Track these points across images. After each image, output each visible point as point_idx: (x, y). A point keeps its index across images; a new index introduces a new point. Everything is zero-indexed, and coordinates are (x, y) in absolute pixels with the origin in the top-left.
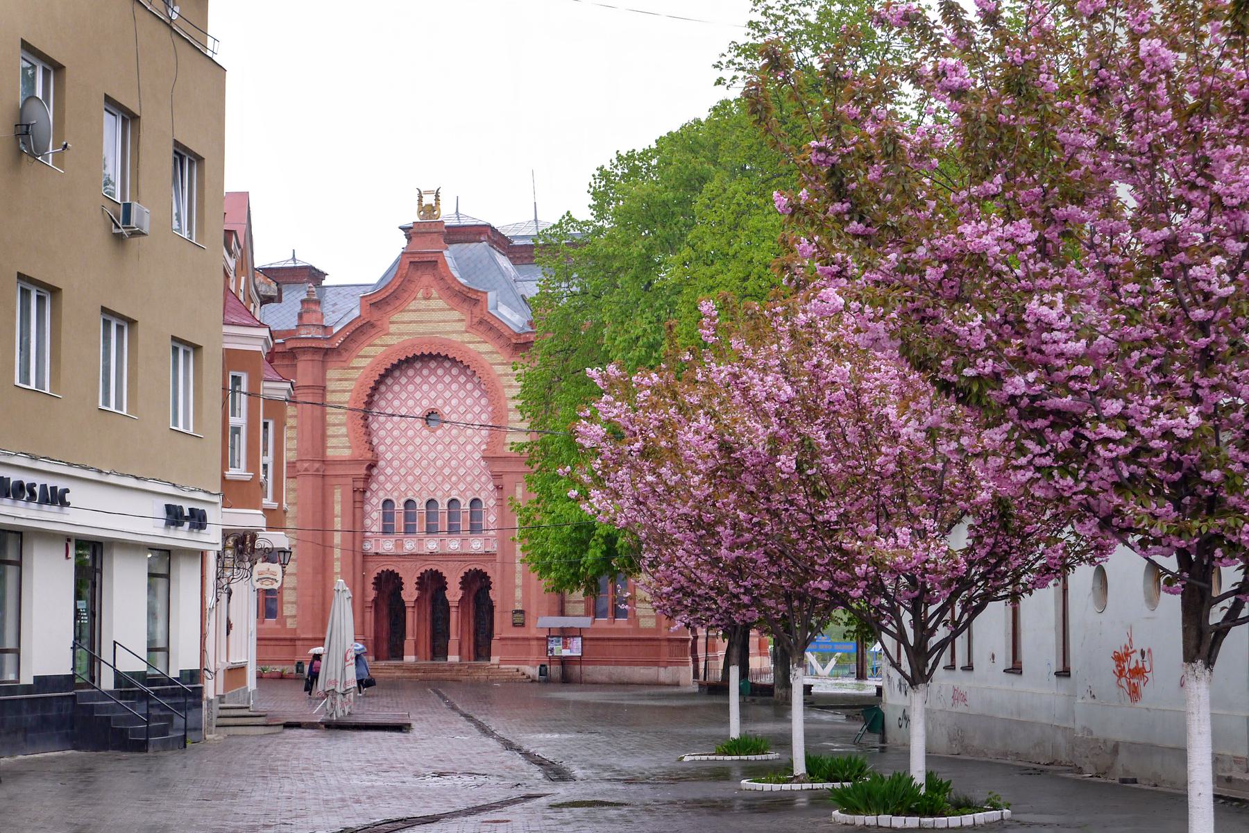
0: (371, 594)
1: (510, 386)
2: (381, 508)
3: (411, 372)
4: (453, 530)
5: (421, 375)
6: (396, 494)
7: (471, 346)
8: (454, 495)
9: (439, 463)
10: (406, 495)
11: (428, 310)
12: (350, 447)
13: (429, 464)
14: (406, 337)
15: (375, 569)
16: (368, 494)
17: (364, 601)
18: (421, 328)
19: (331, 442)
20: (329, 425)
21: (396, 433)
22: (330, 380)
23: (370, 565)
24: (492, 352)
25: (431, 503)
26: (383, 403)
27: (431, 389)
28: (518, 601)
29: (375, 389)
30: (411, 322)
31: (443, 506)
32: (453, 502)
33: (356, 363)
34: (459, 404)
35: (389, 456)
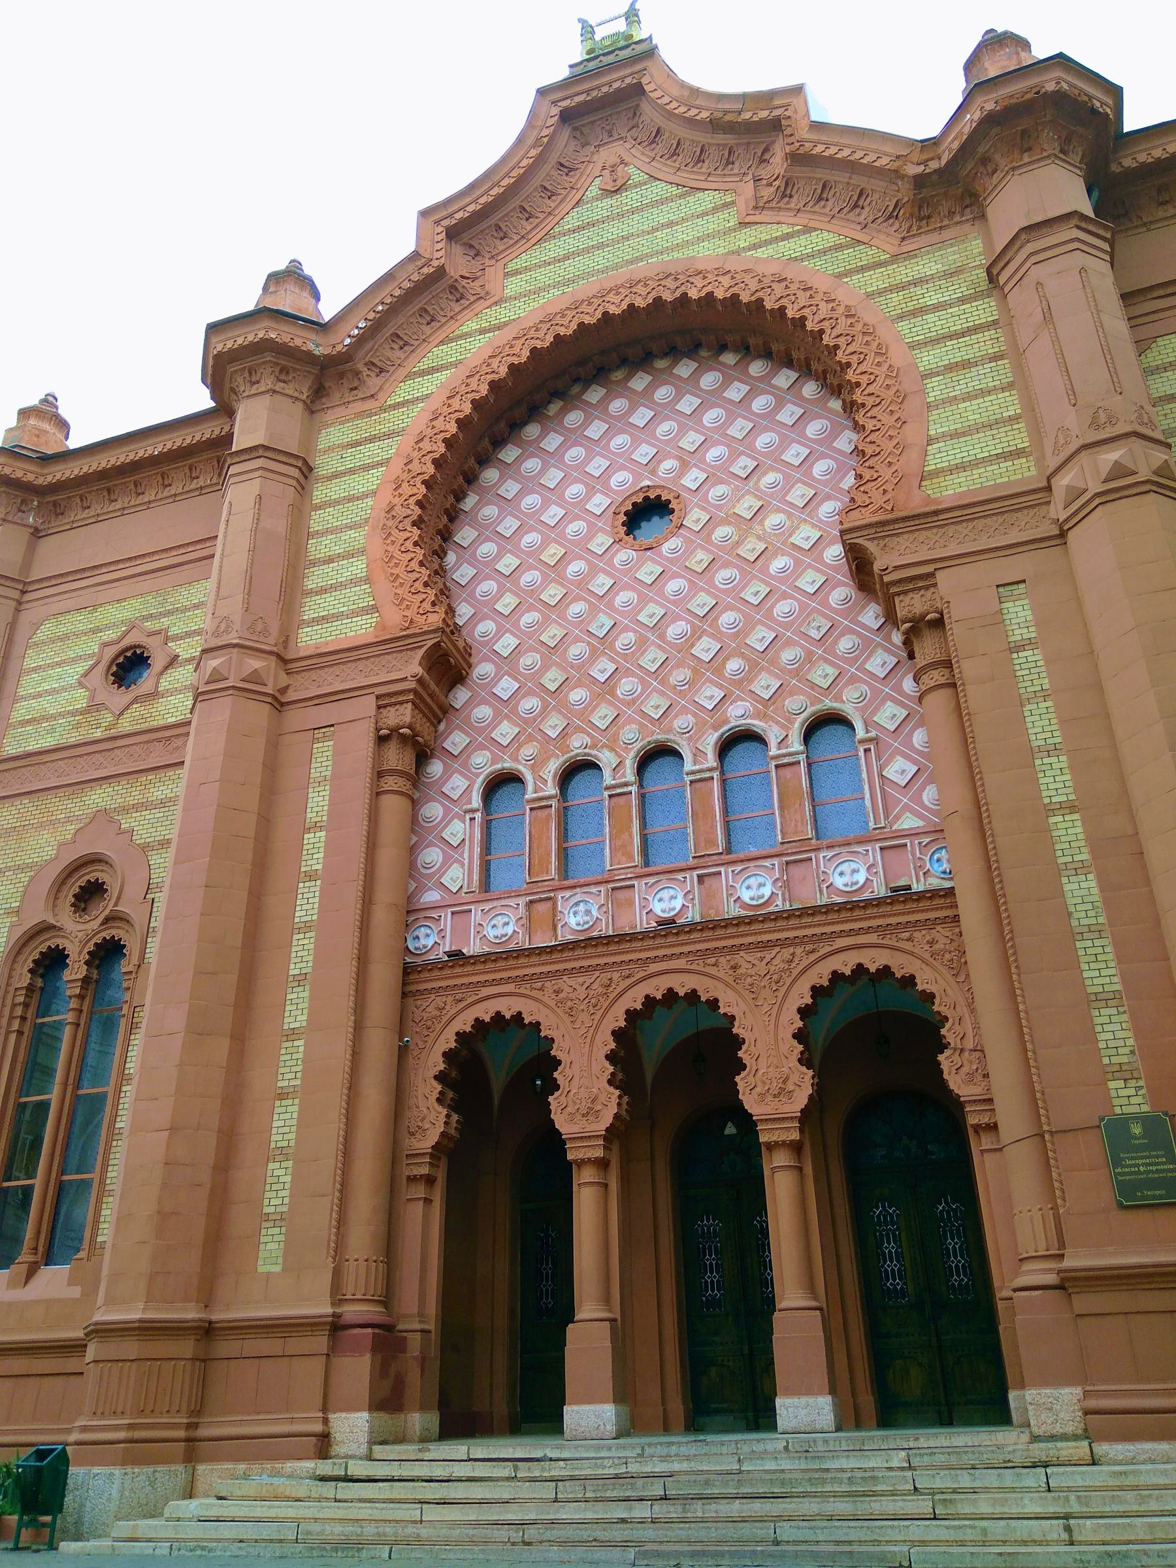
2: (476, 801)
3: (573, 418)
5: (605, 415)
6: (528, 751)
7: (761, 253)
8: (738, 714)
9: (675, 630)
10: (565, 749)
12: (375, 608)
16: (436, 768)
18: (600, 259)
19: (312, 608)
22: (330, 449)
23: (427, 1007)
24: (839, 248)
28: (1125, 1074)
30: (566, 257)
33: (403, 391)
35: (506, 644)
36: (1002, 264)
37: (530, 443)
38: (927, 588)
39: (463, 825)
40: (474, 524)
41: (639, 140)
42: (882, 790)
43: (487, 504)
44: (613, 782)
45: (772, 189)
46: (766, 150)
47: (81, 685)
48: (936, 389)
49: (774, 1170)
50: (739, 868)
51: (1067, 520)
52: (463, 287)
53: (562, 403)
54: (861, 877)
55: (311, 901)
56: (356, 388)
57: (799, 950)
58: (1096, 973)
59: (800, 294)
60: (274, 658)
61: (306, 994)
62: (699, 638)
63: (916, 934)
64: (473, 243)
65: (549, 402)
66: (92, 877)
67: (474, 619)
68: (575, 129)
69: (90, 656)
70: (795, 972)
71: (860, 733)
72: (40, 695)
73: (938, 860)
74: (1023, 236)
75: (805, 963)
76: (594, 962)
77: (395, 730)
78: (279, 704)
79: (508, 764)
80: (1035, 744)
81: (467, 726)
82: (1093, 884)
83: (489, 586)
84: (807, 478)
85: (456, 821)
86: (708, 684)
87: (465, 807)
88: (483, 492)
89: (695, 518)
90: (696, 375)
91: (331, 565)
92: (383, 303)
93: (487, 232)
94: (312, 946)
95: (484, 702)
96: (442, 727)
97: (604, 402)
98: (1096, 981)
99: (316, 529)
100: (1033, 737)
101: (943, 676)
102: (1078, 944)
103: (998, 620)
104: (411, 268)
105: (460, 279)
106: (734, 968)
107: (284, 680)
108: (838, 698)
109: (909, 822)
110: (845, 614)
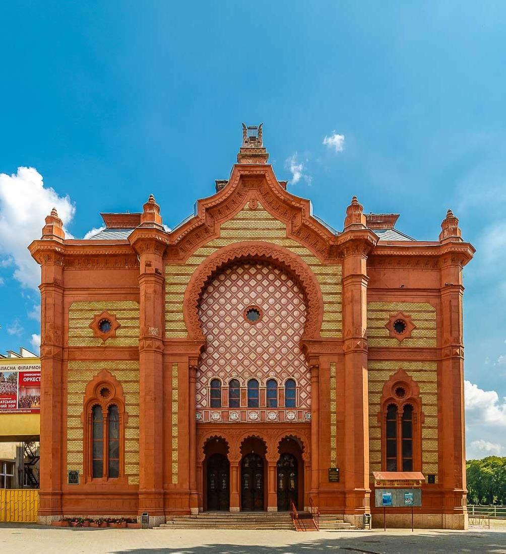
0: (203, 457)
2: (209, 385)
3: (234, 277)
4: (272, 405)
6: (222, 374)
8: (272, 375)
9: (259, 350)
13: (250, 350)
15: (206, 437)
16: (199, 374)
17: (197, 463)
21: (222, 325)
25: (253, 382)
26: (211, 301)
28: (333, 461)
29: (204, 290)
31: (262, 385)
32: (272, 382)
34: (275, 303)
35: (216, 343)
47: (90, 327)
49: (270, 471)
53: (230, 271)
62: (264, 353)
65: (228, 269)
66: (105, 387)
69: (92, 318)
71: (297, 385)
72: (76, 328)
81: (206, 364)
83: (210, 324)
84: (293, 316)
89: (265, 319)
90: (267, 275)
95: (210, 358)
96: (200, 363)
97: (242, 275)
106: (267, 432)
109: (304, 406)
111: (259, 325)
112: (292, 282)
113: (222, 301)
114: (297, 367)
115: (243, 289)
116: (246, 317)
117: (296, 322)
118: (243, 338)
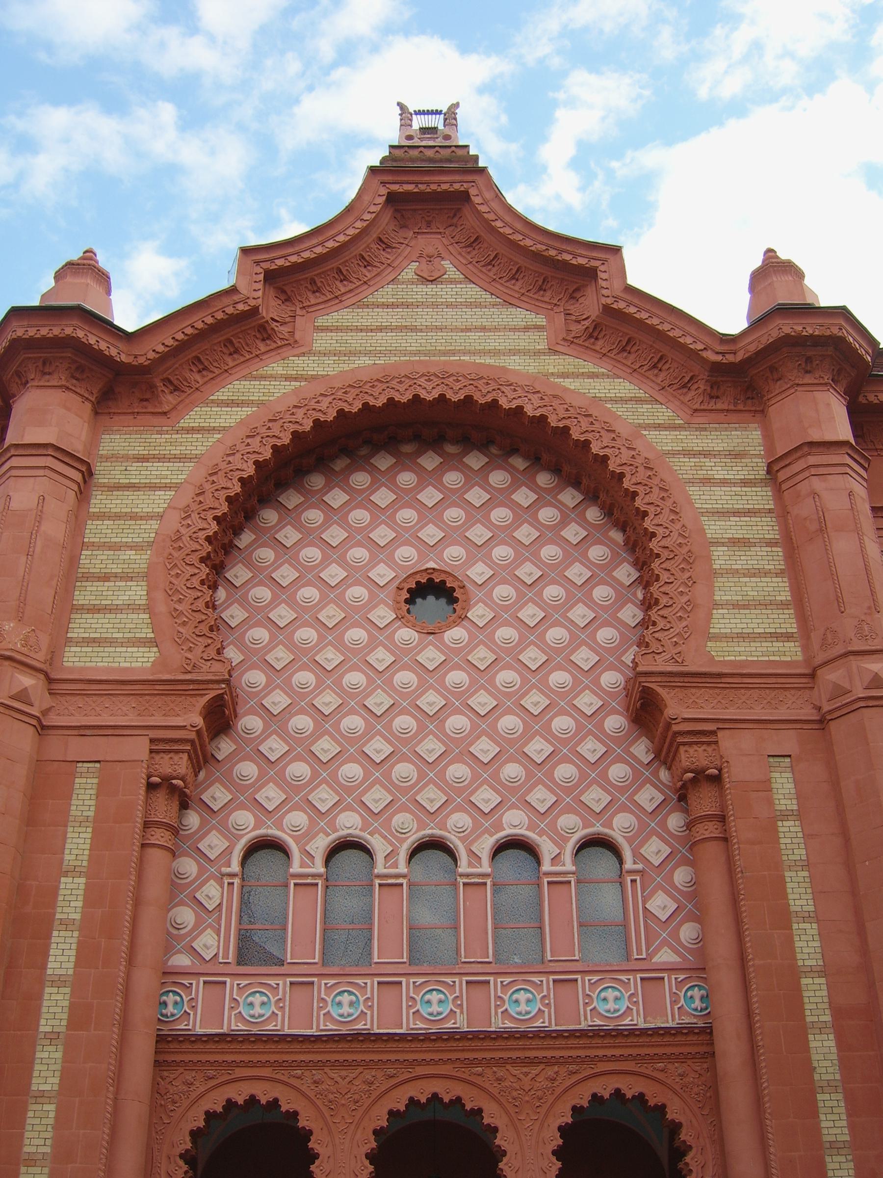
1: (707, 481)
2: (235, 867)
3: (360, 479)
5: (393, 486)
6: (298, 819)
7: (569, 383)
11: (434, 305)
12: (153, 643)
14: (366, 361)
16: (193, 819)
18: (413, 342)
20: (89, 577)
21: (307, 634)
24: (639, 401)
26: (267, 554)
27: (423, 520)
30: (380, 329)
35: (278, 701)
36: (782, 464)
37: (314, 493)
38: (709, 744)
39: (220, 889)
40: (249, 564)
41: (456, 238)
42: (645, 922)
43: (264, 545)
44: (386, 871)
45: (580, 327)
46: (577, 290)
48: (720, 558)
50: (508, 980)
51: (830, 712)
52: (273, 329)
53: (349, 461)
54: (623, 1005)
55: (66, 953)
56: (147, 400)
57: (563, 1071)
58: (831, 1124)
59: (603, 433)
60: (42, 676)
61: (59, 1055)
62: (478, 737)
63: (670, 1066)
64: (286, 288)
67: (245, 665)
68: (396, 210)
70: (559, 1091)
71: (629, 865)
73: (691, 997)
74: (806, 449)
75: (568, 1083)
76: (359, 1057)
77: (166, 779)
78: (42, 729)
79: (274, 832)
80: (793, 909)
82: (833, 1043)
83: (260, 634)
84: (589, 601)
85: (212, 882)
86: (485, 786)
87: (225, 870)
88: (260, 531)
89: (479, 613)
91: (106, 584)
92: (193, 327)
93: (302, 282)
94: (67, 1003)
96: (202, 775)
97: (392, 472)
98: (831, 1131)
99: (91, 540)
100: (791, 902)
101: (717, 829)
102: (819, 1097)
103: (766, 786)
104: (226, 301)
105: (270, 321)
107: (48, 701)
108: (609, 824)
109: (666, 956)
110: (617, 741)
111: (456, 634)
112: (576, 493)
113: (312, 554)
114: (622, 790)
115: (392, 517)
116: (405, 607)
117: (606, 624)
118: (389, 682)
